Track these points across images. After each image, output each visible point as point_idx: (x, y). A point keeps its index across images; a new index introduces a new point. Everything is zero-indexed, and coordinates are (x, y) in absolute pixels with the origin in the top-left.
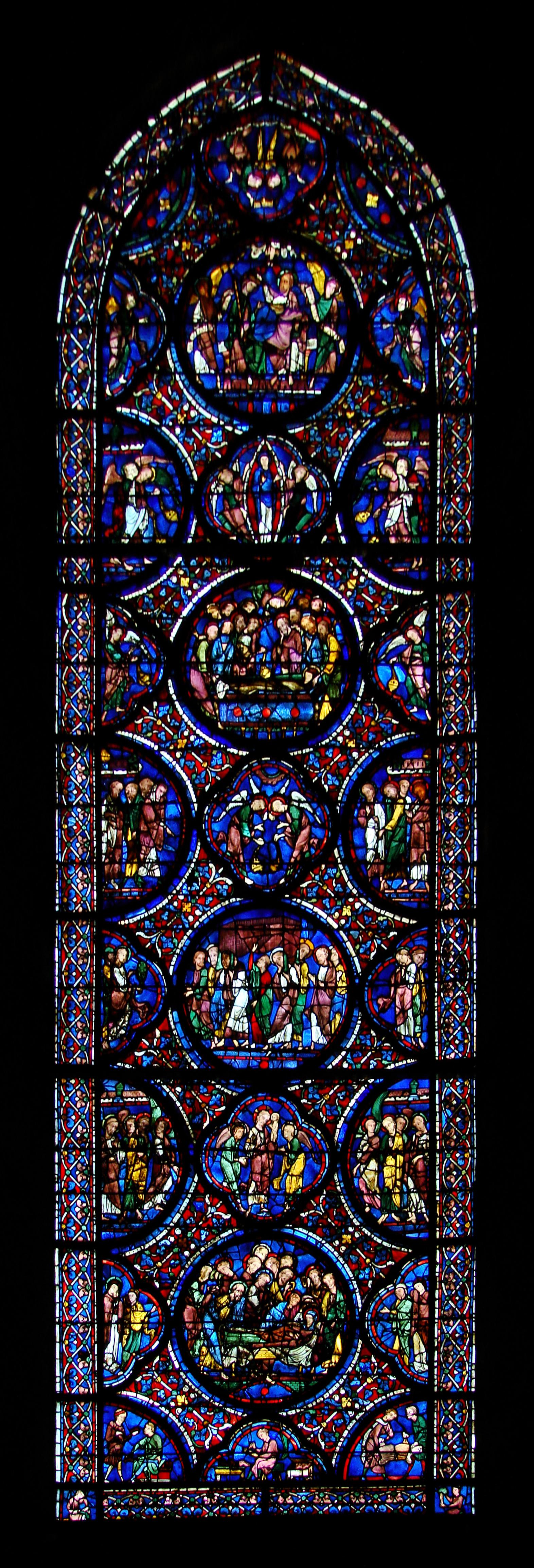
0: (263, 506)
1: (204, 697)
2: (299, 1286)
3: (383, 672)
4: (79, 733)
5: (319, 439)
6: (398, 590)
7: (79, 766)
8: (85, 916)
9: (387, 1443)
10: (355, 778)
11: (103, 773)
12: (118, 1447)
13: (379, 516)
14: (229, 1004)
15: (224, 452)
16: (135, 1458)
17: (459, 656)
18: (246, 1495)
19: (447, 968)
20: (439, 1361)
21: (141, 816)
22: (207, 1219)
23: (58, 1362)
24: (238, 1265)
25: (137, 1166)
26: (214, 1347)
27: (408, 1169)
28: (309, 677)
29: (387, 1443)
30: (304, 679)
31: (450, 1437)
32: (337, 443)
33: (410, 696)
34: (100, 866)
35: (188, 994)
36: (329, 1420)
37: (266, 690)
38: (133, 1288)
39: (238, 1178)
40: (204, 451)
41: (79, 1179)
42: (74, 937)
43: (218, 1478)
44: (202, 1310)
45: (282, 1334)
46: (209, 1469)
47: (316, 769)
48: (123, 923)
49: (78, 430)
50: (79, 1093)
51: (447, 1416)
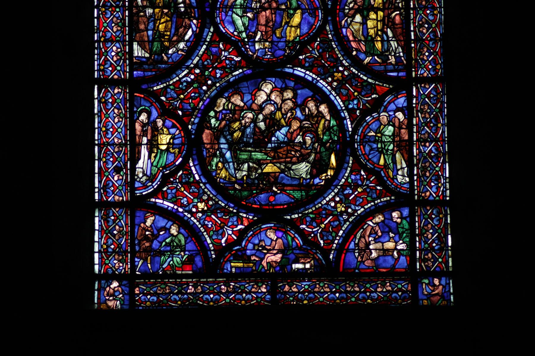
2: (299, 114)
12: (147, 244)
16: (162, 253)
20: (418, 174)
22: (221, 61)
23: (97, 175)
24: (247, 97)
25: (163, 20)
26: (229, 163)
27: (388, 22)
29: (376, 241)
31: (430, 236)
36: (326, 222)
38: (160, 116)
39: (246, 29)
43: (234, 270)
44: (217, 133)
45: (286, 153)
46: (226, 262)
51: (426, 220)
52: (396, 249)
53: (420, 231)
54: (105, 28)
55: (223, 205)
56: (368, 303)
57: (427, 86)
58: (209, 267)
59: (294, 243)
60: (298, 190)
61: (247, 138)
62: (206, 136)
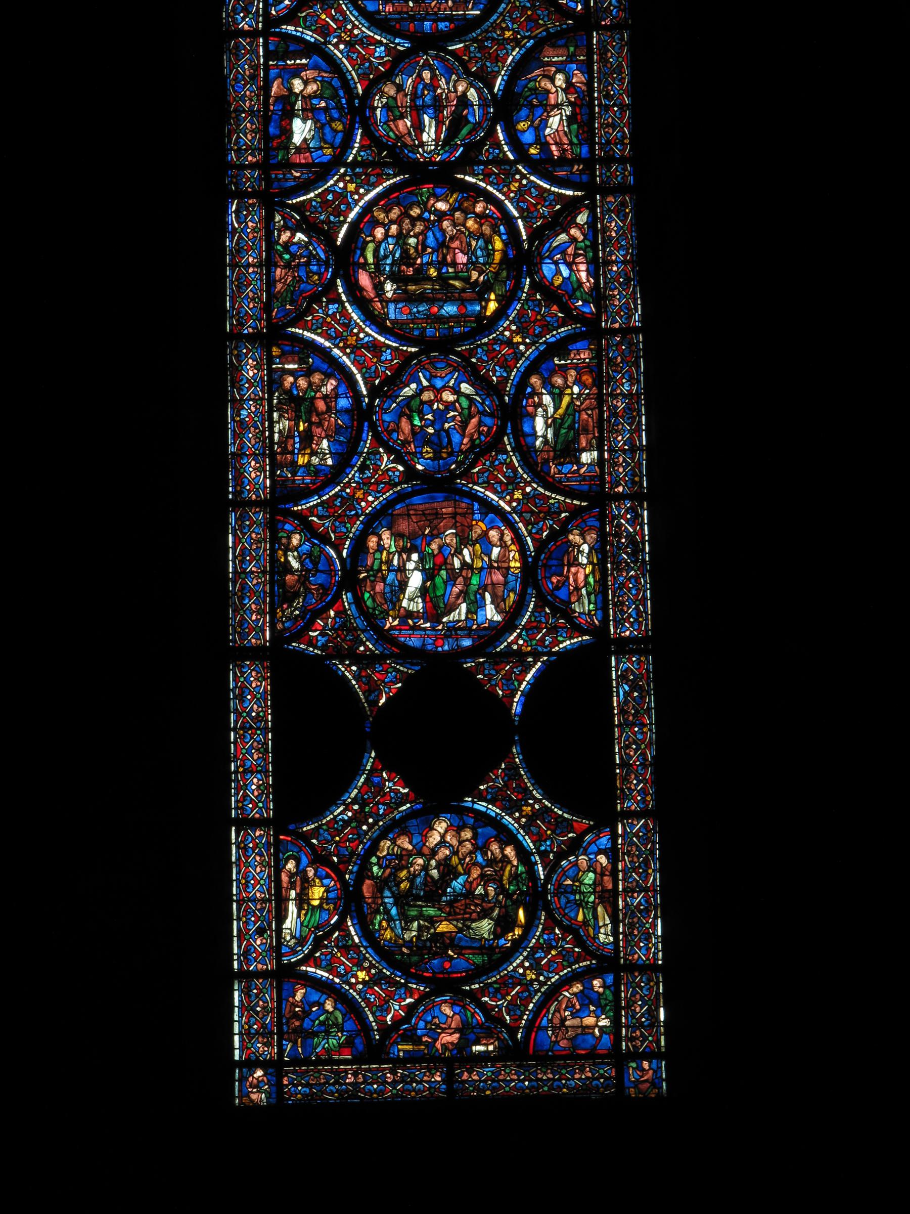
0: (426, 118)
1: (372, 295)
2: (480, 859)
3: (548, 269)
4: (251, 330)
5: (479, 55)
6: (560, 191)
7: (250, 361)
8: (258, 503)
9: (574, 1015)
10: (522, 369)
11: (274, 366)
12: (297, 1023)
13: (539, 125)
14: (403, 585)
15: (388, 67)
16: (315, 1034)
17: (621, 252)
18: (429, 1071)
19: (619, 548)
21: (312, 409)
22: (385, 794)
23: (235, 939)
26: (394, 921)
28: (475, 275)
29: (574, 1015)
30: (470, 277)
31: (638, 1009)
32: (498, 59)
33: (574, 290)
34: (273, 455)
35: (363, 575)
36: (513, 993)
37: (433, 289)
38: (311, 863)
40: (367, 65)
41: (255, 757)
42: (248, 523)
43: (401, 1054)
44: (381, 884)
45: (465, 907)
46: (392, 1045)
47: (483, 361)
48: (296, 509)
49: (245, 48)
50: (254, 674)
51: (634, 989)
52: (597, 1026)
53: (627, 1002)
54: (244, 755)
55: (388, 973)
56: (564, 1093)
57: (635, 823)
58: (371, 1049)
59: (474, 1020)
60: (479, 954)
61: (417, 889)
62: (367, 888)
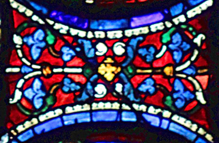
47: (27, 54)
